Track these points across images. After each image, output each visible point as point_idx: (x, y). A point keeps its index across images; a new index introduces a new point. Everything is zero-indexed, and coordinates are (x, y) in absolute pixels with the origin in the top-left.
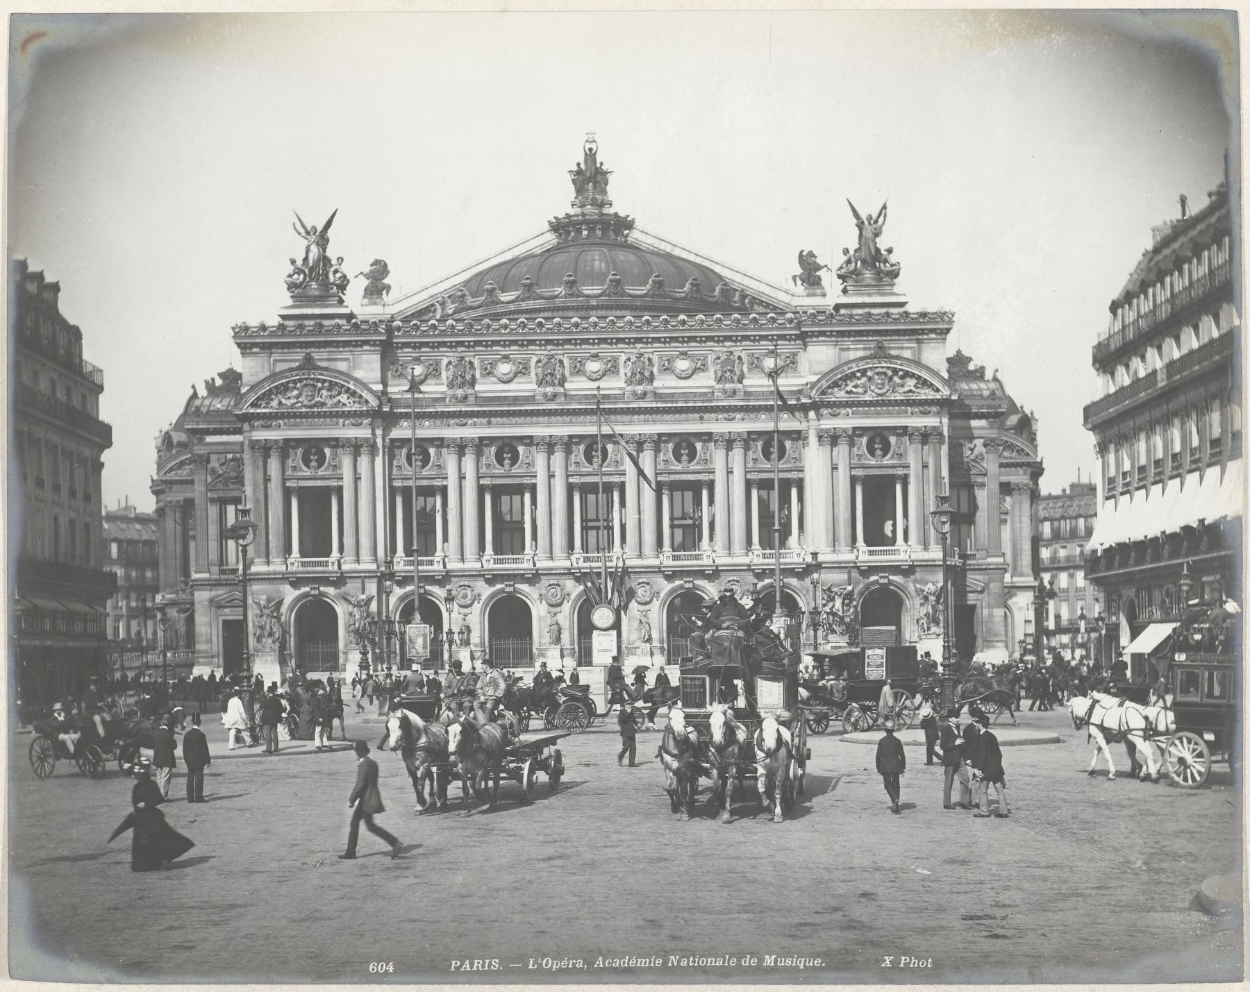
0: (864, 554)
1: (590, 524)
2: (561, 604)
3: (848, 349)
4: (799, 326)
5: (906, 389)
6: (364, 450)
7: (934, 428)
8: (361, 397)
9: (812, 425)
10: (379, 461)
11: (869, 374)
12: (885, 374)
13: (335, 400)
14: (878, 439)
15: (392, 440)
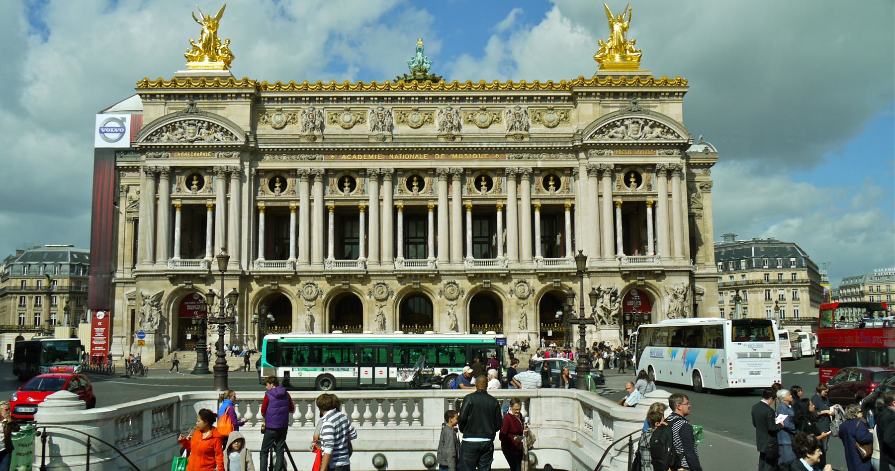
0: (627, 263)
1: (411, 240)
2: (386, 299)
3: (609, 107)
4: (571, 89)
5: (654, 134)
6: (233, 176)
7: (677, 165)
8: (232, 134)
9: (581, 163)
10: (246, 186)
11: (626, 122)
12: (637, 122)
13: (212, 137)
14: (633, 173)
15: (258, 171)
